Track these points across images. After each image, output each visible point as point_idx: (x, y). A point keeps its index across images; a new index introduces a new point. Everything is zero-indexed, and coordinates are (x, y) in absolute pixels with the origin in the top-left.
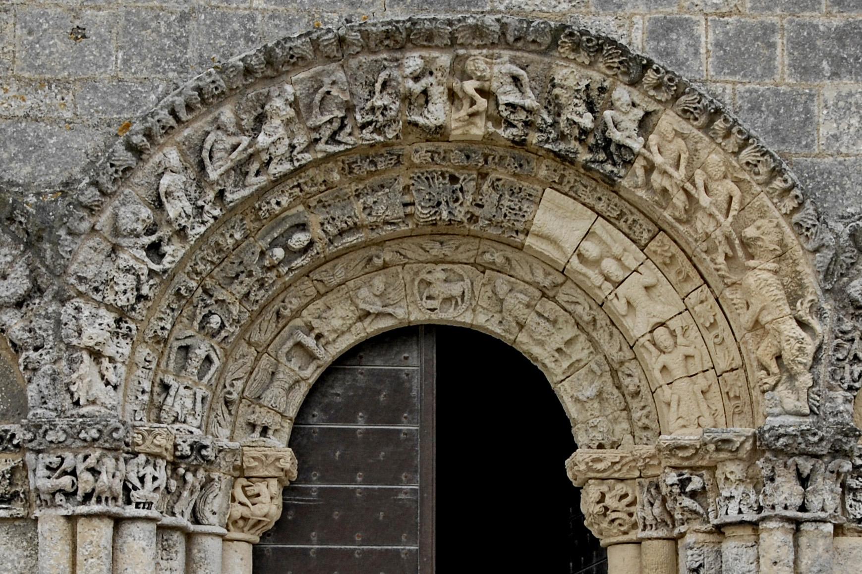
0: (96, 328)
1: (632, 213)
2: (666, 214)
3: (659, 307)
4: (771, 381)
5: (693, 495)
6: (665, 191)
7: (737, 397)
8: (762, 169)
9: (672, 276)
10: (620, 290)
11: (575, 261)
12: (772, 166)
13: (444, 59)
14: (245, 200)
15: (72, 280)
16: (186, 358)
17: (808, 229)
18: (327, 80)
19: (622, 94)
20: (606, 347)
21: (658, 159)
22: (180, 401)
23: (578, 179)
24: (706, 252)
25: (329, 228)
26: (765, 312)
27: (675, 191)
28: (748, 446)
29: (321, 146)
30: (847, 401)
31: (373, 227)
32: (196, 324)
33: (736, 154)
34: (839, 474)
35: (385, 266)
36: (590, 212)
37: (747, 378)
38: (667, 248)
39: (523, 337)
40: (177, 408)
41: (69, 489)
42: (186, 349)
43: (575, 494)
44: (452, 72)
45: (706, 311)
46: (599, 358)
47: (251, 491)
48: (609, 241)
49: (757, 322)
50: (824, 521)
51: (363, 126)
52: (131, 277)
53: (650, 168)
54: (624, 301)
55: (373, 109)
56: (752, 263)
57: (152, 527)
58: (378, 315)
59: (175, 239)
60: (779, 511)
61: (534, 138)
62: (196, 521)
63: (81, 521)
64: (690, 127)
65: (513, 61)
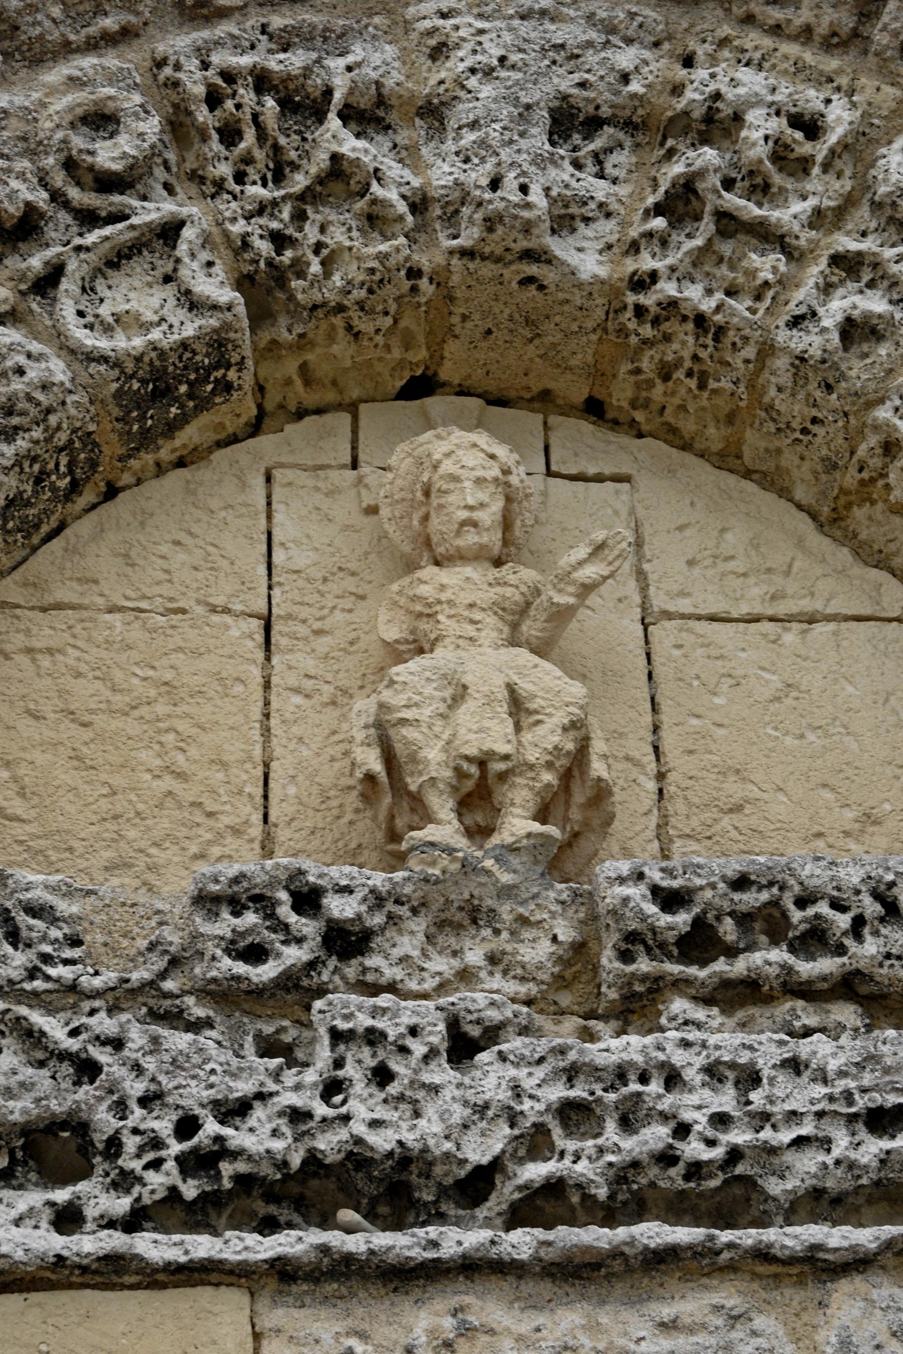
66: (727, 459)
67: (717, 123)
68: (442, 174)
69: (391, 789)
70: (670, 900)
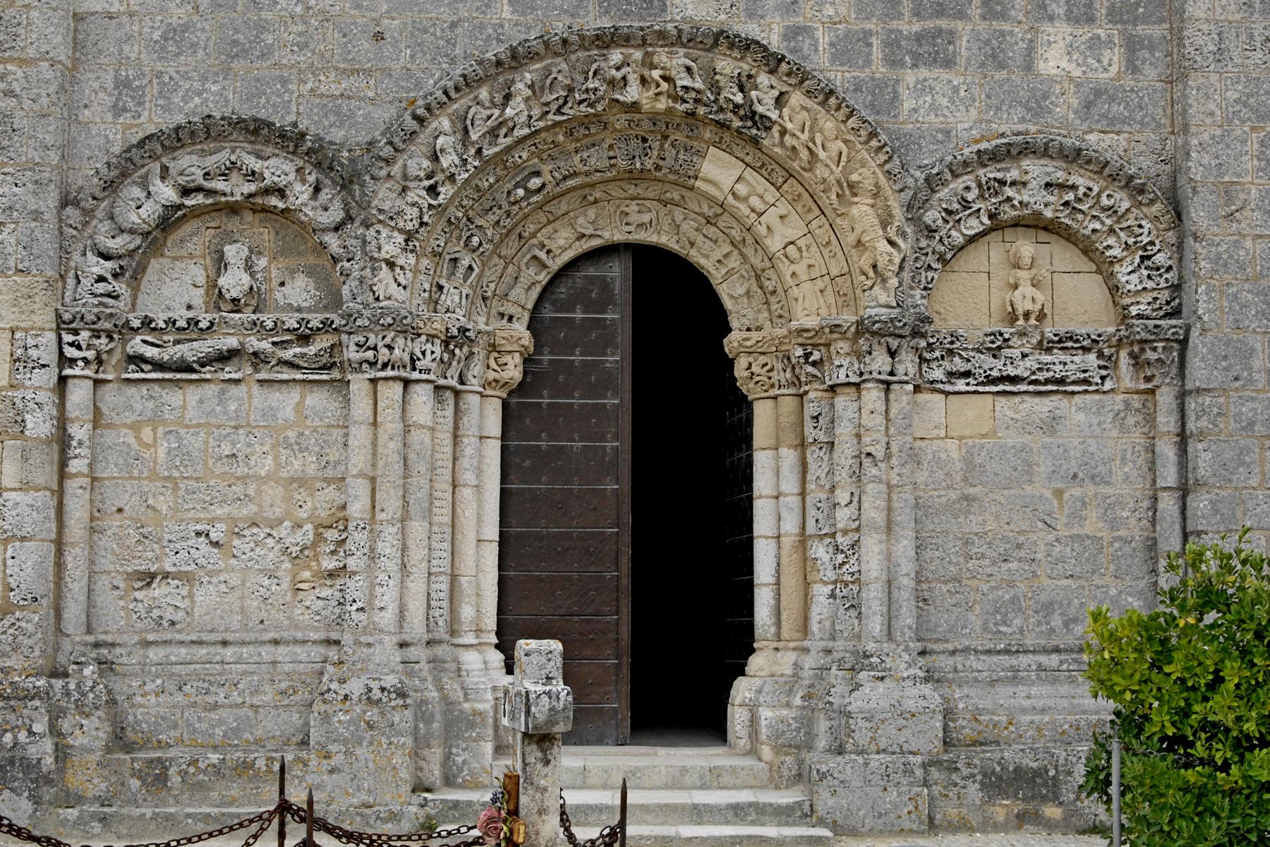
0: (391, 245)
3: (790, 231)
4: (869, 283)
5: (814, 364)
6: (794, 148)
7: (845, 295)
8: (863, 133)
9: (799, 209)
10: (762, 219)
11: (730, 198)
13: (638, 55)
14: (496, 154)
15: (374, 212)
16: (455, 267)
18: (555, 70)
19: (763, 79)
20: (752, 259)
21: (789, 126)
22: (451, 297)
25: (556, 174)
28: (853, 329)
29: (550, 116)
30: (923, 297)
31: (587, 174)
32: (462, 243)
33: (844, 122)
34: (917, 349)
35: (596, 201)
39: (693, 252)
40: (449, 302)
41: (372, 359)
42: (455, 260)
43: (730, 364)
44: (643, 64)
45: (823, 233)
46: (748, 266)
47: (501, 361)
48: (754, 184)
49: (859, 241)
50: (907, 383)
51: (580, 102)
52: (416, 209)
53: (783, 132)
54: (765, 226)
55: (587, 90)
56: (855, 199)
57: (431, 386)
58: (591, 236)
59: (447, 183)
60: (875, 375)
61: (701, 110)
62: (462, 382)
63: (381, 382)
65: (686, 56)
66: (1068, 240)
67: (1074, 187)
68: (1026, 199)
69: (1012, 318)
70: (1055, 335)
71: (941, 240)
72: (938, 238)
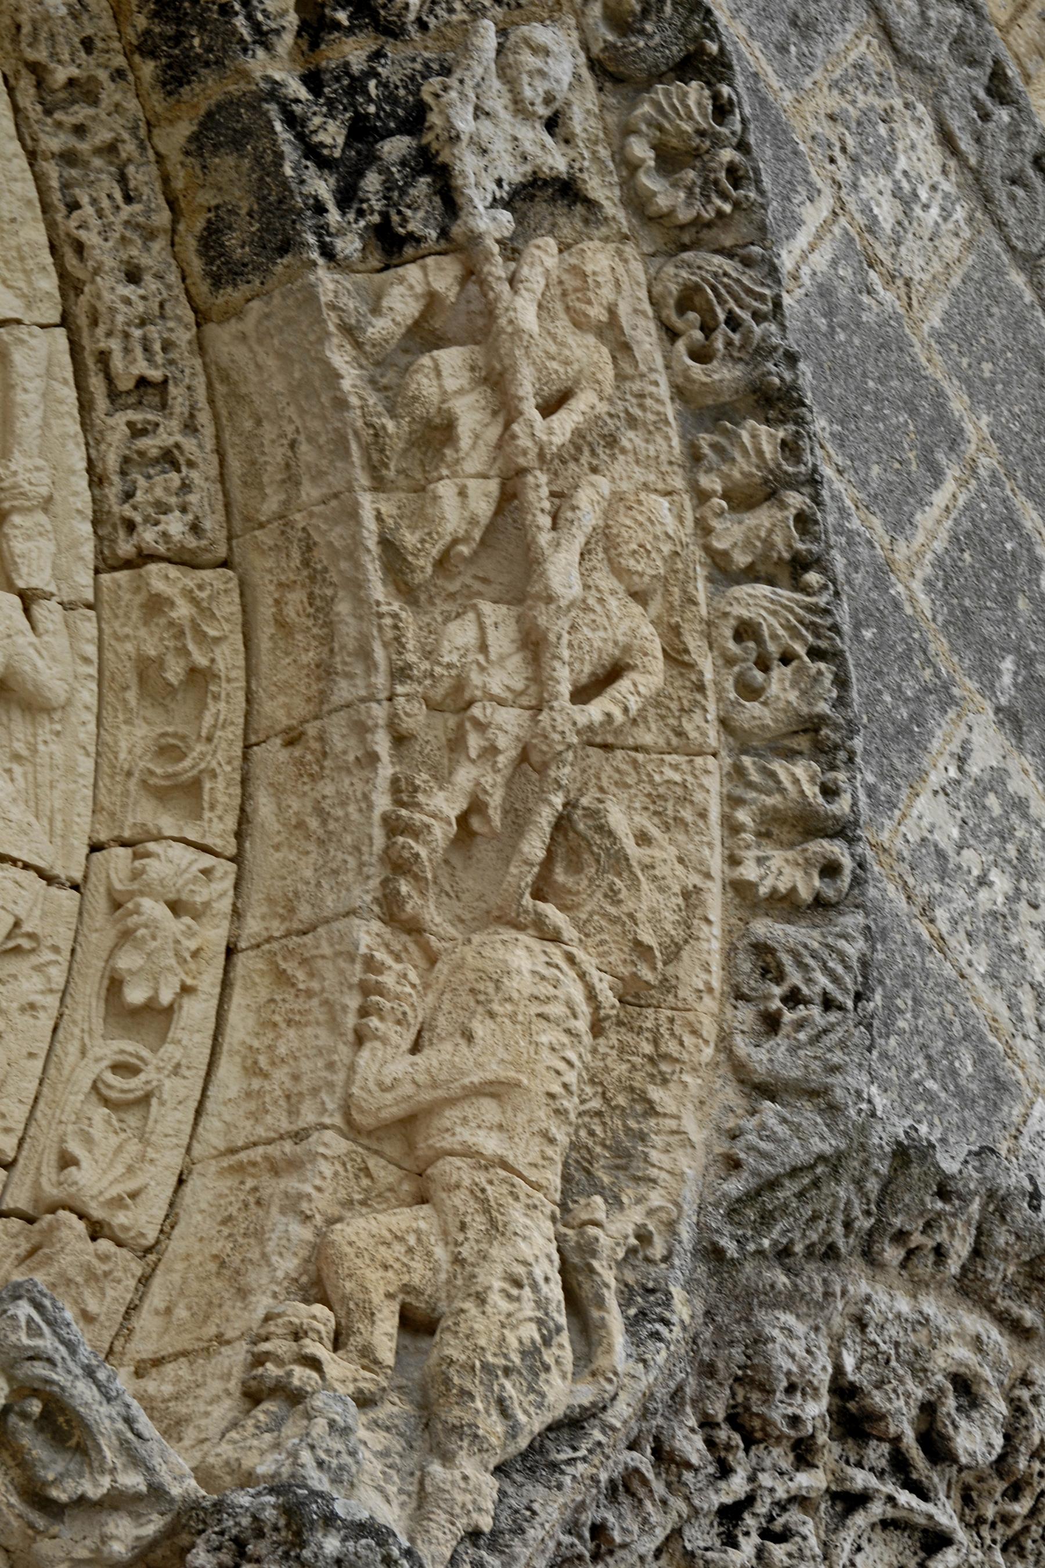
1: (190, 427)
2: (368, 504)
6: (437, 434)
8: (780, 685)
9: (134, 739)
12: (823, 707)
17: (794, 998)
23: (129, 148)
24: (400, 740)
26: (489, 1110)
27: (473, 464)
33: (724, 572)
36: (49, 283)
37: (132, 1309)
38: (212, 633)
45: (174, 955)
56: (549, 909)
64: (659, 362)
71: (730, 1515)
72: (737, 1486)
